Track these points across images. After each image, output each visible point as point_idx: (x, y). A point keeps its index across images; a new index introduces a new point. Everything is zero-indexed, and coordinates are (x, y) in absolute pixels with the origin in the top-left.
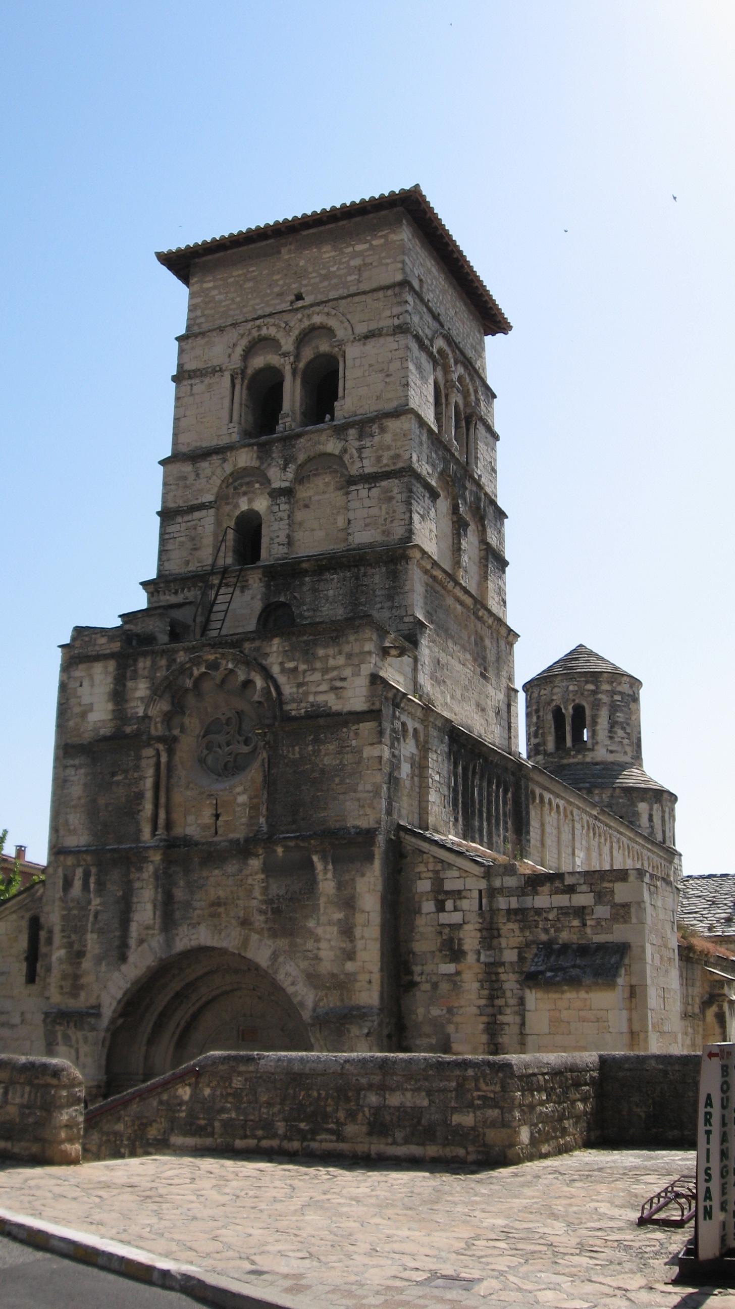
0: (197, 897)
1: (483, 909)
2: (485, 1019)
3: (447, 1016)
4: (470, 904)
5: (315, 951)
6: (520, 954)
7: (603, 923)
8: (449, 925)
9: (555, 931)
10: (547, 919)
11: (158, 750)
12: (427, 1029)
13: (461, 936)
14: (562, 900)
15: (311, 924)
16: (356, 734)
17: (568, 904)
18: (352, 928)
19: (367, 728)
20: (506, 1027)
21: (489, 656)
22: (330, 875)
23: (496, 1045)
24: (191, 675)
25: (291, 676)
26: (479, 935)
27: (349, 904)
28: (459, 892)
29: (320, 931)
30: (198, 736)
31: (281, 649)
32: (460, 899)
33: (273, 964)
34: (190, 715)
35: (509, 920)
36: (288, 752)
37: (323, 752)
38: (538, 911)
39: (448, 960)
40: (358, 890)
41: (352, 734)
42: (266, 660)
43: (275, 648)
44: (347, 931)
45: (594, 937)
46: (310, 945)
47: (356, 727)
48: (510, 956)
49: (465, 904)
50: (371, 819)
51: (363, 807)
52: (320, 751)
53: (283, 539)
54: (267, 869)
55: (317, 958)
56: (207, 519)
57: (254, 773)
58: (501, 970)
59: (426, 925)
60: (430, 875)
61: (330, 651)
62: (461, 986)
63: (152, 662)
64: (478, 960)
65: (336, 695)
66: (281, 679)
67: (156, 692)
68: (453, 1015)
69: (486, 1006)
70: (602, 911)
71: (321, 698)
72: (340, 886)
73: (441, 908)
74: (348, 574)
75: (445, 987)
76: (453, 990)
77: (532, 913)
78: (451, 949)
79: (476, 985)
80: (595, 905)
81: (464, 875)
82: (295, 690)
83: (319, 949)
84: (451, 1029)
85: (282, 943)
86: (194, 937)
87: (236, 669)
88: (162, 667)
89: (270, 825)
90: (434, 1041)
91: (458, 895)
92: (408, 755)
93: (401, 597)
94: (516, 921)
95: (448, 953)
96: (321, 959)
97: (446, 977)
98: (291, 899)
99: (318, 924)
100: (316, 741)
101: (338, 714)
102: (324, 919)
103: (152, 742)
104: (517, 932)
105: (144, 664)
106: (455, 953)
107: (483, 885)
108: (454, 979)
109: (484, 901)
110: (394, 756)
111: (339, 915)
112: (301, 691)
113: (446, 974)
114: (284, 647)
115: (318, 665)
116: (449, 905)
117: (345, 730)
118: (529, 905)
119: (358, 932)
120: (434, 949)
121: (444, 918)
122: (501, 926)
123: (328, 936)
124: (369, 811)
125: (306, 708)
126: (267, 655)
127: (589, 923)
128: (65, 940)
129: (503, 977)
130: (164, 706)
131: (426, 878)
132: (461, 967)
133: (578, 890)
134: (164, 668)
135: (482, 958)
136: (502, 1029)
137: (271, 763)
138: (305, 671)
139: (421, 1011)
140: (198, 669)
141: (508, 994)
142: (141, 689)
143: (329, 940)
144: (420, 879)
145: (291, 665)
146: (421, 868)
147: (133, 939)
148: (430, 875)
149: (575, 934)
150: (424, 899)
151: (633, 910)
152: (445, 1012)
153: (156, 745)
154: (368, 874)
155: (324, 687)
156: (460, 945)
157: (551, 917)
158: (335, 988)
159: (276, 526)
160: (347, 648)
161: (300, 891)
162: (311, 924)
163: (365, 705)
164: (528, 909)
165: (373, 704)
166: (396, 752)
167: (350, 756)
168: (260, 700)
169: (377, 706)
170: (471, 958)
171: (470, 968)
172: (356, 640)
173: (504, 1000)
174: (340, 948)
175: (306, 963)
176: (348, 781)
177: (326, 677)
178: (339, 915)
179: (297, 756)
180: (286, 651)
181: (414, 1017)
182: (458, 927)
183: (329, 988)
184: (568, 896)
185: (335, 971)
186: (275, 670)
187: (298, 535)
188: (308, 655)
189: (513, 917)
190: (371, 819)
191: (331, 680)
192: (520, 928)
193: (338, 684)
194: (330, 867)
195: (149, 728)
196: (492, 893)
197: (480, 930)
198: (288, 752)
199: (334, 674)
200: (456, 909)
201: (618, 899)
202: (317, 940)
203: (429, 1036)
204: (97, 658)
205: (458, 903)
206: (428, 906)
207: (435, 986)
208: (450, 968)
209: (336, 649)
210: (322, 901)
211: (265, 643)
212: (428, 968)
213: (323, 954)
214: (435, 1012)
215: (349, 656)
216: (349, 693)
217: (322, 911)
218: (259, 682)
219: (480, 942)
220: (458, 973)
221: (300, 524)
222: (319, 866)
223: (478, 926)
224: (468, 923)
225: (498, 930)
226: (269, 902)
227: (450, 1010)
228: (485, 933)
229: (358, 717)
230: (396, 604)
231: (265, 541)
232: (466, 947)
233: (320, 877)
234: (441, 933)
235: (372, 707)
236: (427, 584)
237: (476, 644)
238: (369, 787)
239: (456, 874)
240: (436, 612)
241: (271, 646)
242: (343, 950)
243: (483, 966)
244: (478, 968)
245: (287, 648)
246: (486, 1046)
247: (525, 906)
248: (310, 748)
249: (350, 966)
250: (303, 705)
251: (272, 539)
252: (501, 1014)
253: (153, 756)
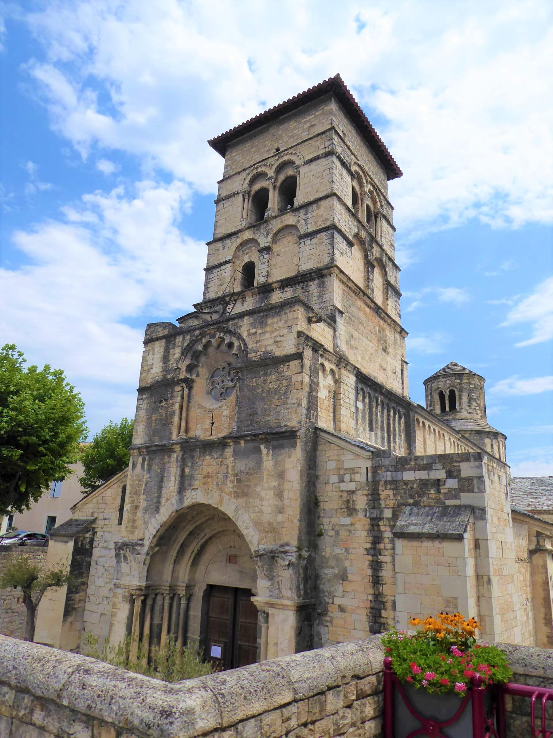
0: (197, 472)
1: (369, 480)
2: (370, 558)
3: (345, 554)
4: (361, 477)
5: (260, 507)
6: (393, 511)
7: (453, 492)
8: (348, 492)
9: (419, 497)
10: (412, 488)
12: (332, 563)
13: (355, 499)
14: (422, 475)
15: (258, 489)
16: (288, 368)
17: (427, 478)
18: (282, 492)
19: (294, 364)
20: (384, 565)
21: (388, 340)
22: (270, 457)
23: (378, 577)
26: (366, 498)
27: (281, 476)
28: (353, 469)
29: (263, 494)
32: (354, 473)
33: (236, 514)
34: (202, 367)
35: (385, 489)
36: (250, 382)
37: (269, 381)
38: (406, 483)
39: (346, 514)
40: (286, 467)
41: (286, 368)
43: (245, 322)
44: (279, 494)
45: (446, 501)
46: (257, 503)
47: (288, 364)
48: (388, 514)
49: (357, 477)
50: (295, 421)
51: (291, 413)
52: (267, 380)
53: (265, 274)
54: (236, 454)
55: (261, 511)
56: (228, 269)
57: (233, 397)
58: (381, 523)
59: (332, 491)
60: (335, 457)
61: (275, 320)
62: (354, 534)
64: (365, 516)
65: (277, 345)
66: (247, 339)
67: (184, 353)
68: (349, 554)
69: (371, 548)
70: (452, 483)
71: (269, 348)
72: (276, 464)
73: (342, 480)
74: (298, 287)
75: (343, 534)
76: (349, 535)
77: (402, 484)
78: (348, 508)
79: (364, 533)
80: (446, 479)
81: (357, 457)
82: (255, 345)
83: (262, 506)
84: (347, 564)
85: (242, 501)
86: (194, 497)
89: (238, 427)
90: (336, 571)
91: (353, 471)
92: (327, 385)
93: (327, 295)
94: (391, 489)
95: (346, 510)
96: (263, 512)
97: (346, 527)
98: (248, 473)
99: (262, 489)
100: (266, 374)
101: (277, 357)
102: (266, 485)
104: (392, 497)
105: (179, 339)
106: (351, 510)
107: (369, 464)
108: (350, 529)
109: (370, 475)
110: (312, 381)
111: (275, 484)
112: (258, 345)
113: (344, 525)
115: (268, 329)
116: (347, 478)
117: (282, 366)
118: (399, 478)
119: (286, 495)
120: (337, 508)
121: (344, 486)
122: (380, 492)
123: (268, 497)
124: (294, 415)
125: (261, 355)
126: (241, 326)
127: (442, 491)
128: (131, 499)
129: (382, 528)
130: (188, 362)
131: (333, 460)
132: (354, 519)
133: (434, 468)
135: (368, 515)
136: (381, 567)
137: (241, 390)
138: (261, 333)
139: (328, 550)
141: (386, 541)
142: (176, 353)
143: (269, 500)
144: (329, 460)
145: (253, 331)
146: (329, 453)
147: (164, 499)
148: (335, 457)
149: (432, 499)
150: (332, 473)
151: (475, 482)
152: (344, 550)
154: (293, 456)
155: (271, 341)
156: (353, 505)
157: (415, 486)
158: (271, 532)
159: (261, 267)
160: (284, 317)
161: (253, 468)
162: (258, 489)
163: (294, 350)
164: (399, 481)
165: (298, 349)
166: (315, 380)
167: (284, 382)
168: (237, 353)
169: (301, 351)
170: (361, 515)
171: (360, 521)
172: (290, 312)
173: (382, 545)
174: (275, 505)
175: (255, 514)
176: (282, 397)
177: (272, 336)
178: (275, 484)
179: (255, 384)
181: (323, 554)
182: (353, 492)
183: (267, 532)
184: (427, 472)
185: (271, 521)
186: (244, 335)
187: (273, 272)
188: (263, 324)
189: (389, 486)
190: (295, 421)
191: (275, 337)
192: (393, 494)
193: (279, 339)
194: (271, 452)
196: (375, 469)
197: (367, 495)
198: (250, 382)
199: (276, 333)
200: (351, 481)
201: (464, 474)
202: (262, 500)
203: (333, 568)
204: (158, 339)
205: (353, 476)
206: (334, 479)
207: (337, 533)
208: (348, 521)
209: (279, 318)
210: (265, 474)
211: (240, 320)
212: (334, 520)
213: (264, 509)
214: (338, 551)
215: (286, 322)
216: (285, 344)
217: (265, 481)
218: (236, 344)
219: (367, 504)
220: (352, 524)
221: (275, 265)
222: (264, 451)
223: (365, 492)
224: (359, 490)
225: (379, 495)
226: (236, 475)
227: (347, 550)
228: (370, 497)
229: (288, 358)
230: (324, 300)
231: (256, 276)
232: (358, 507)
233: (265, 458)
234: (341, 497)
235: (298, 351)
236: (344, 290)
237: (379, 332)
238: (294, 401)
239: (351, 456)
240: (350, 307)
242: (276, 506)
243: (368, 520)
244: (366, 522)
246: (371, 577)
247: (395, 479)
248: (262, 378)
249: (280, 517)
250: (259, 353)
251: (259, 274)
252: (380, 555)
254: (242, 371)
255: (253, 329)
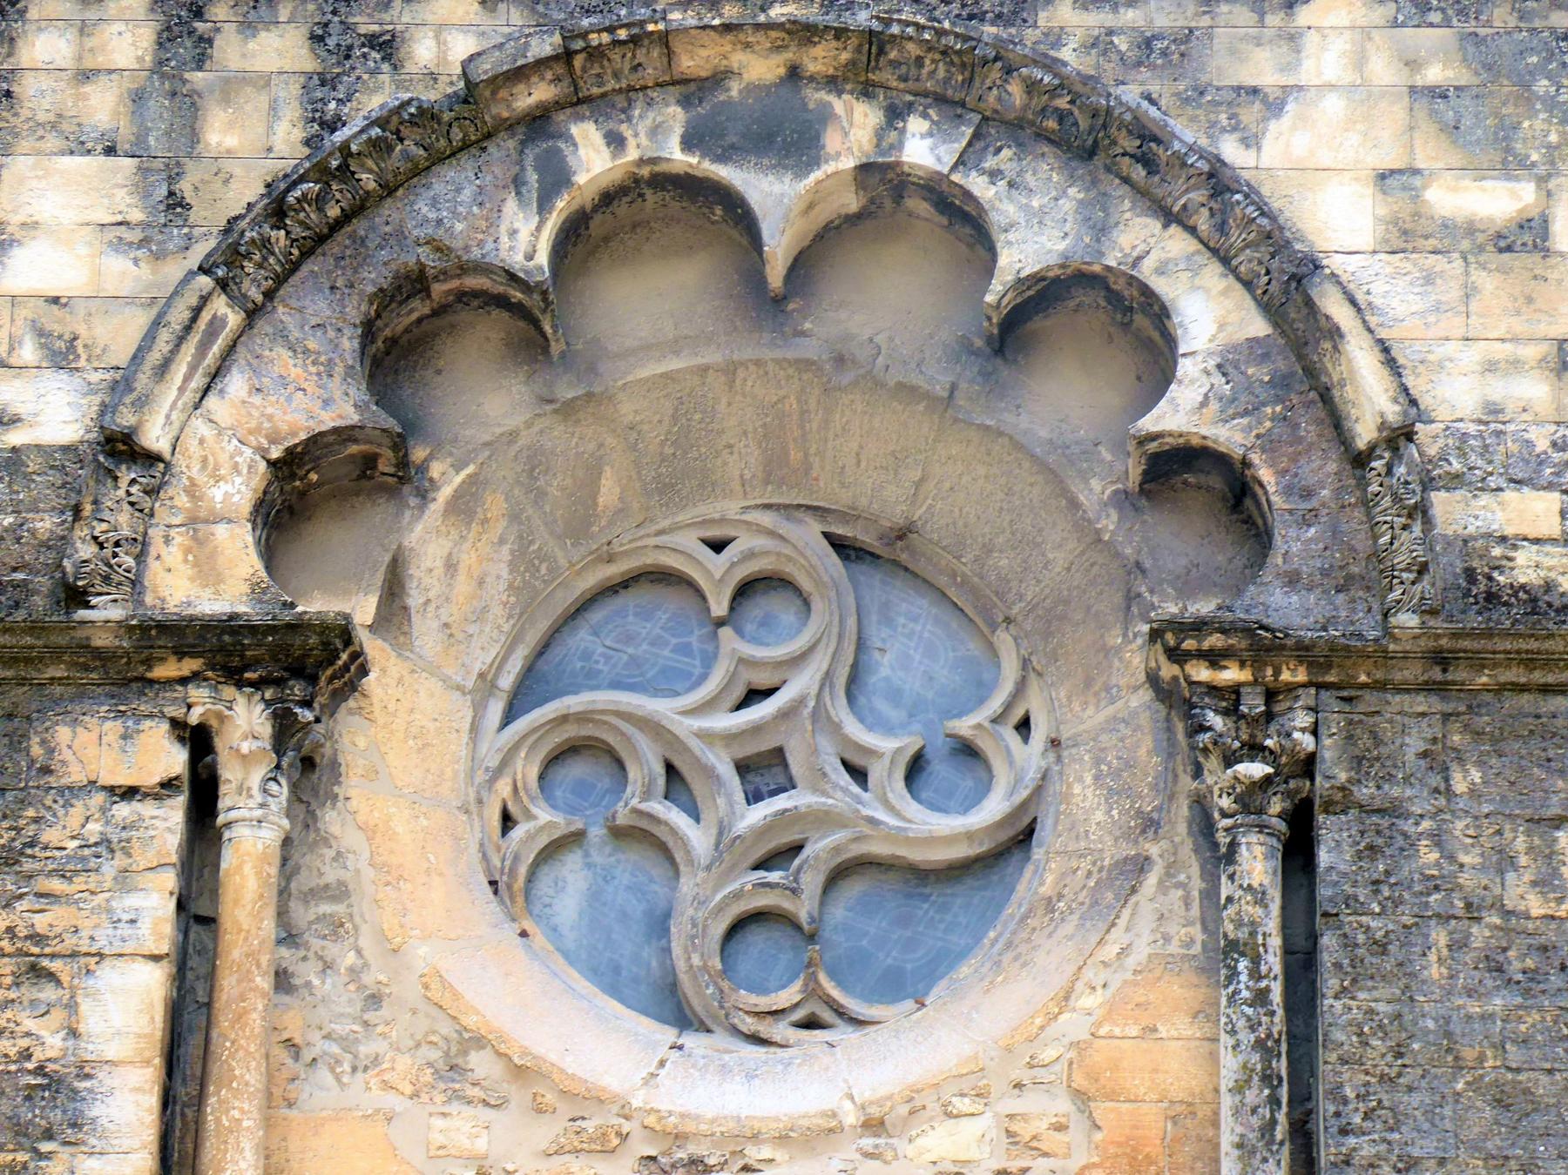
11: (199, 740)
24: (556, 178)
25: (1487, 282)
30: (486, 681)
31: (1383, 70)
42: (1251, 141)
63: (166, 38)
87: (977, 184)
88: (264, 81)
103: (168, 669)
114: (1413, 64)
134: (290, 95)
140: (616, 142)
153: (198, 693)
168: (1230, 437)
180: (1438, 93)
195: (141, 547)
198: (1504, 862)
241: (1293, 39)
245: (1435, 74)
253: (169, 785)
254: (1348, 693)
255: (1479, 172)
